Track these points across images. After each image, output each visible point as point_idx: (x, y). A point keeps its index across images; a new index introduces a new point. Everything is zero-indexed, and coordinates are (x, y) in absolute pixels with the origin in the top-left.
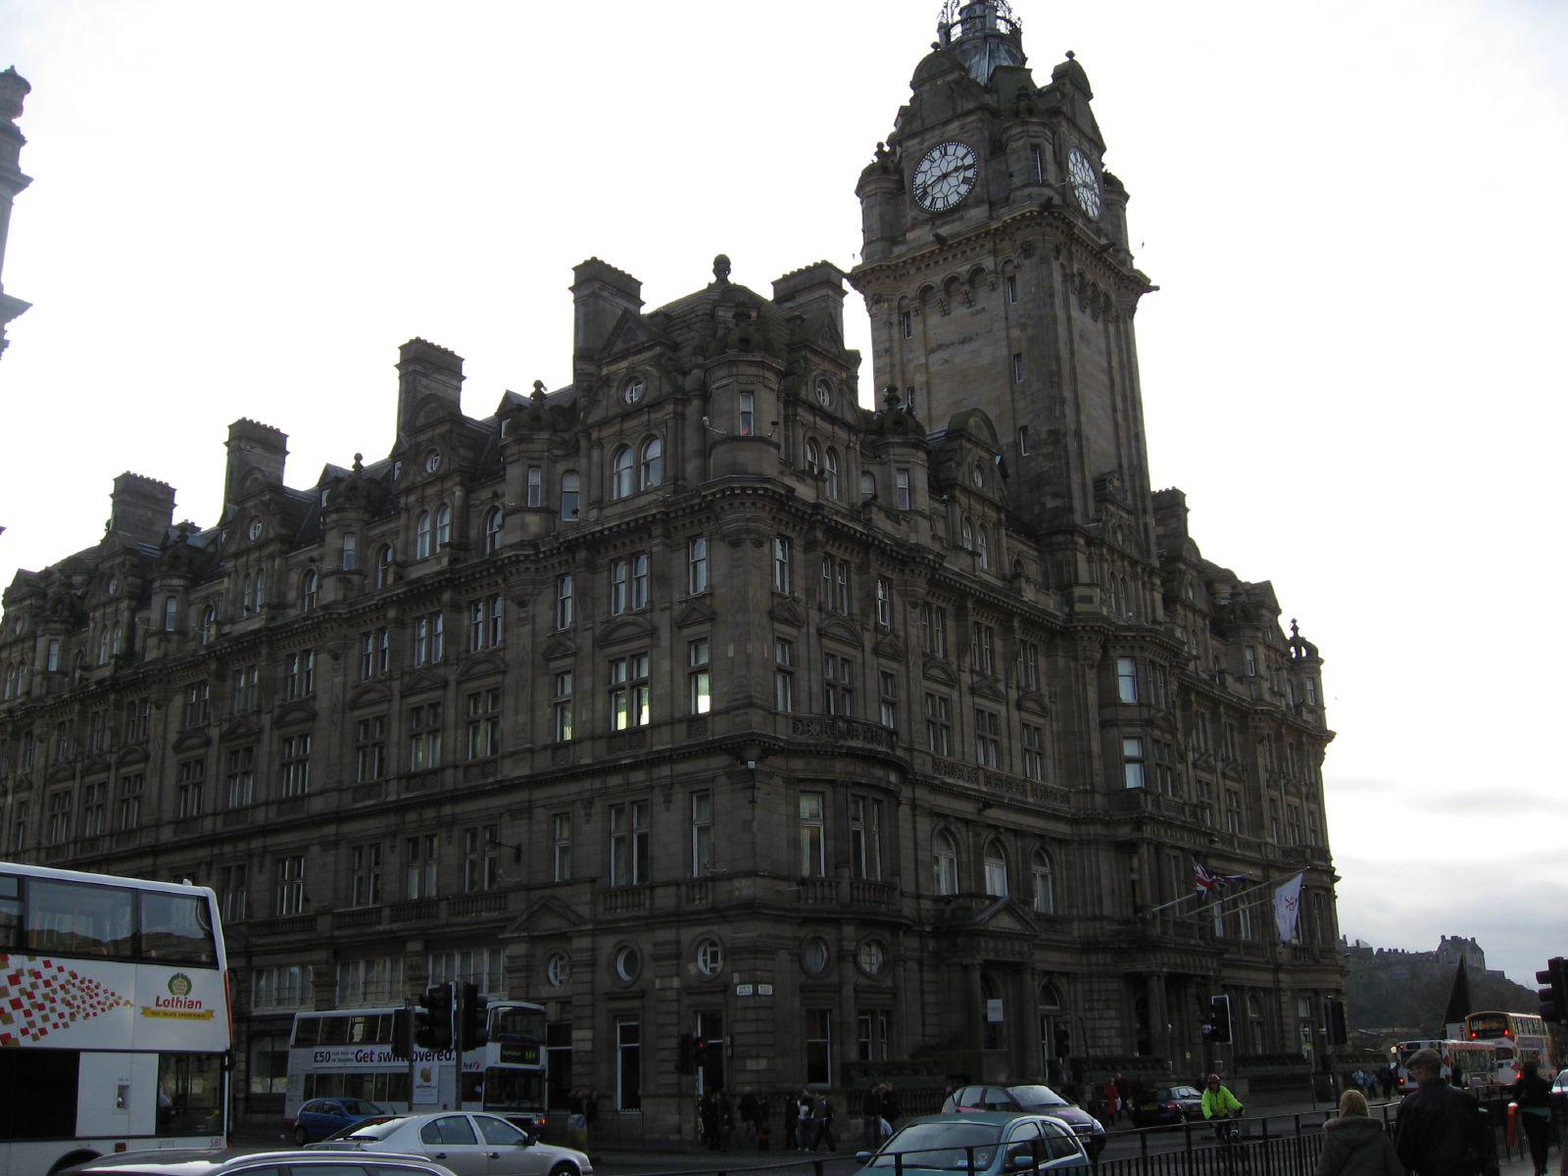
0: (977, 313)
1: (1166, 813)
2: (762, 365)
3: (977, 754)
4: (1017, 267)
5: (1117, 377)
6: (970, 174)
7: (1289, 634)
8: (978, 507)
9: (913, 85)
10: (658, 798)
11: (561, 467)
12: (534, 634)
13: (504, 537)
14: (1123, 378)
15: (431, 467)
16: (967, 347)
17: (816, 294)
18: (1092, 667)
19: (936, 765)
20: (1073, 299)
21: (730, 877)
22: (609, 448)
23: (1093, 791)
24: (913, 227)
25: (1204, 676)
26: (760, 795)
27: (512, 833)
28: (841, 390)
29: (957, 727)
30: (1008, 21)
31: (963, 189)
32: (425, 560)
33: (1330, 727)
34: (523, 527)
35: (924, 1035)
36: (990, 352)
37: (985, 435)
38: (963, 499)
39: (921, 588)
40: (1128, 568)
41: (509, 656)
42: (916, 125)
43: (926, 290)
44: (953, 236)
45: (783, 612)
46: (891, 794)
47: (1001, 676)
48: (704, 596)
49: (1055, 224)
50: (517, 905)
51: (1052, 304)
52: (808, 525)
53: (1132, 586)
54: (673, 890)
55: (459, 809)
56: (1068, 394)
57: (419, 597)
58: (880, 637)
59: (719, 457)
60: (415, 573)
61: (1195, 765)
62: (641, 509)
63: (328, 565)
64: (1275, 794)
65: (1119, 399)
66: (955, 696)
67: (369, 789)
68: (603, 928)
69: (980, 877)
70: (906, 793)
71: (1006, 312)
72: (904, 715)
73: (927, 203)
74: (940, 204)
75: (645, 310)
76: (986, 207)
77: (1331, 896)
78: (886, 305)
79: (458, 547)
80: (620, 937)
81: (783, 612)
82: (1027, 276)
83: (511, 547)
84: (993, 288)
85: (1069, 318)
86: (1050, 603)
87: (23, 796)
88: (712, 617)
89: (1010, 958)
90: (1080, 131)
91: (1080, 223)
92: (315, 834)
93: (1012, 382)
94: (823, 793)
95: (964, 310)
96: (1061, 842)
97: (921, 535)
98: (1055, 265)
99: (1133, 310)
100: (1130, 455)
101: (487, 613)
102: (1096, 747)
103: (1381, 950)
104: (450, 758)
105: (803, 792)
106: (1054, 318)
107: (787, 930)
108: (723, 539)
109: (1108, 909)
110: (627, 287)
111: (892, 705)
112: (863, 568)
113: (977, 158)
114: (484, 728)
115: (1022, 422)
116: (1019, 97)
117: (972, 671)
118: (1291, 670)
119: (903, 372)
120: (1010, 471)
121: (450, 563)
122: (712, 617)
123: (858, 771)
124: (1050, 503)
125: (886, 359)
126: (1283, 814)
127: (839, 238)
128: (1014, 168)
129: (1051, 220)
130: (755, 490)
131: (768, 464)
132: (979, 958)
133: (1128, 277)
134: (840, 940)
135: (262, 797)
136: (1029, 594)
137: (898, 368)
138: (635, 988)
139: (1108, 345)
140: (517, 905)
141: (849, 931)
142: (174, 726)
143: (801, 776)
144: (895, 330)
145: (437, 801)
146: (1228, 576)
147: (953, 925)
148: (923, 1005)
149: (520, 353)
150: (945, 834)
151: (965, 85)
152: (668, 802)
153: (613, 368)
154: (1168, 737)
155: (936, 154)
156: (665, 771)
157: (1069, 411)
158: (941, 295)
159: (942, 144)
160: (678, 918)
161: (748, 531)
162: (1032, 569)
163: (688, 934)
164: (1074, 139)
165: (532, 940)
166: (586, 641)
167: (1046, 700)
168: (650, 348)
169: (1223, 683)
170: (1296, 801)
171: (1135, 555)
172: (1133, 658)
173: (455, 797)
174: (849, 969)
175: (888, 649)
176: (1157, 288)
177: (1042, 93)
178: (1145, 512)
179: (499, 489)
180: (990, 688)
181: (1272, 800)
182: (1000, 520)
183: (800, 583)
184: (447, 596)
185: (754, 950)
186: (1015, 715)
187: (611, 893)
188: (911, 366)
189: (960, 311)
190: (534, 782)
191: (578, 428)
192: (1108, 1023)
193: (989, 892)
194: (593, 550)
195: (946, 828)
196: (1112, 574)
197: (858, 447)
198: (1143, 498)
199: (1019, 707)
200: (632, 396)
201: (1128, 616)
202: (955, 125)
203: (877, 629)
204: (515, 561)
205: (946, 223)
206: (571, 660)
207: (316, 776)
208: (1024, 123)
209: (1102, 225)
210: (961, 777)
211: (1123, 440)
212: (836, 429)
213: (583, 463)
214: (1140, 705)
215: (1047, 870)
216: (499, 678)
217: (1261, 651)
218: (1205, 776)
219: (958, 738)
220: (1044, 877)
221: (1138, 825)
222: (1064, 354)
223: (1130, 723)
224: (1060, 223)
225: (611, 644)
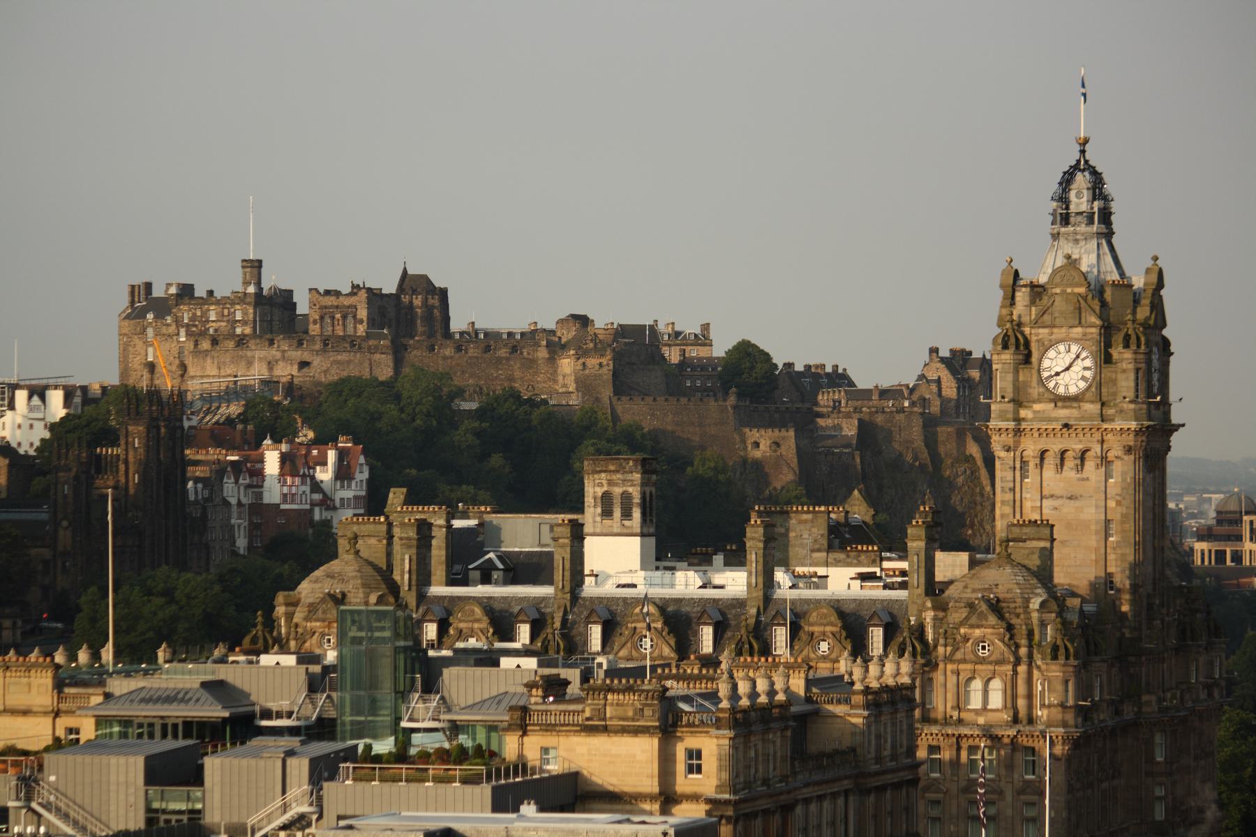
24: (1039, 401)
36: (1091, 513)
74: (1061, 391)
95: (1073, 474)
103: (789, 365)
137: (1018, 504)
144: (1018, 474)
155: (1061, 347)
189: (1069, 472)
202: (1079, 330)
205: (1064, 407)
206: (941, 795)
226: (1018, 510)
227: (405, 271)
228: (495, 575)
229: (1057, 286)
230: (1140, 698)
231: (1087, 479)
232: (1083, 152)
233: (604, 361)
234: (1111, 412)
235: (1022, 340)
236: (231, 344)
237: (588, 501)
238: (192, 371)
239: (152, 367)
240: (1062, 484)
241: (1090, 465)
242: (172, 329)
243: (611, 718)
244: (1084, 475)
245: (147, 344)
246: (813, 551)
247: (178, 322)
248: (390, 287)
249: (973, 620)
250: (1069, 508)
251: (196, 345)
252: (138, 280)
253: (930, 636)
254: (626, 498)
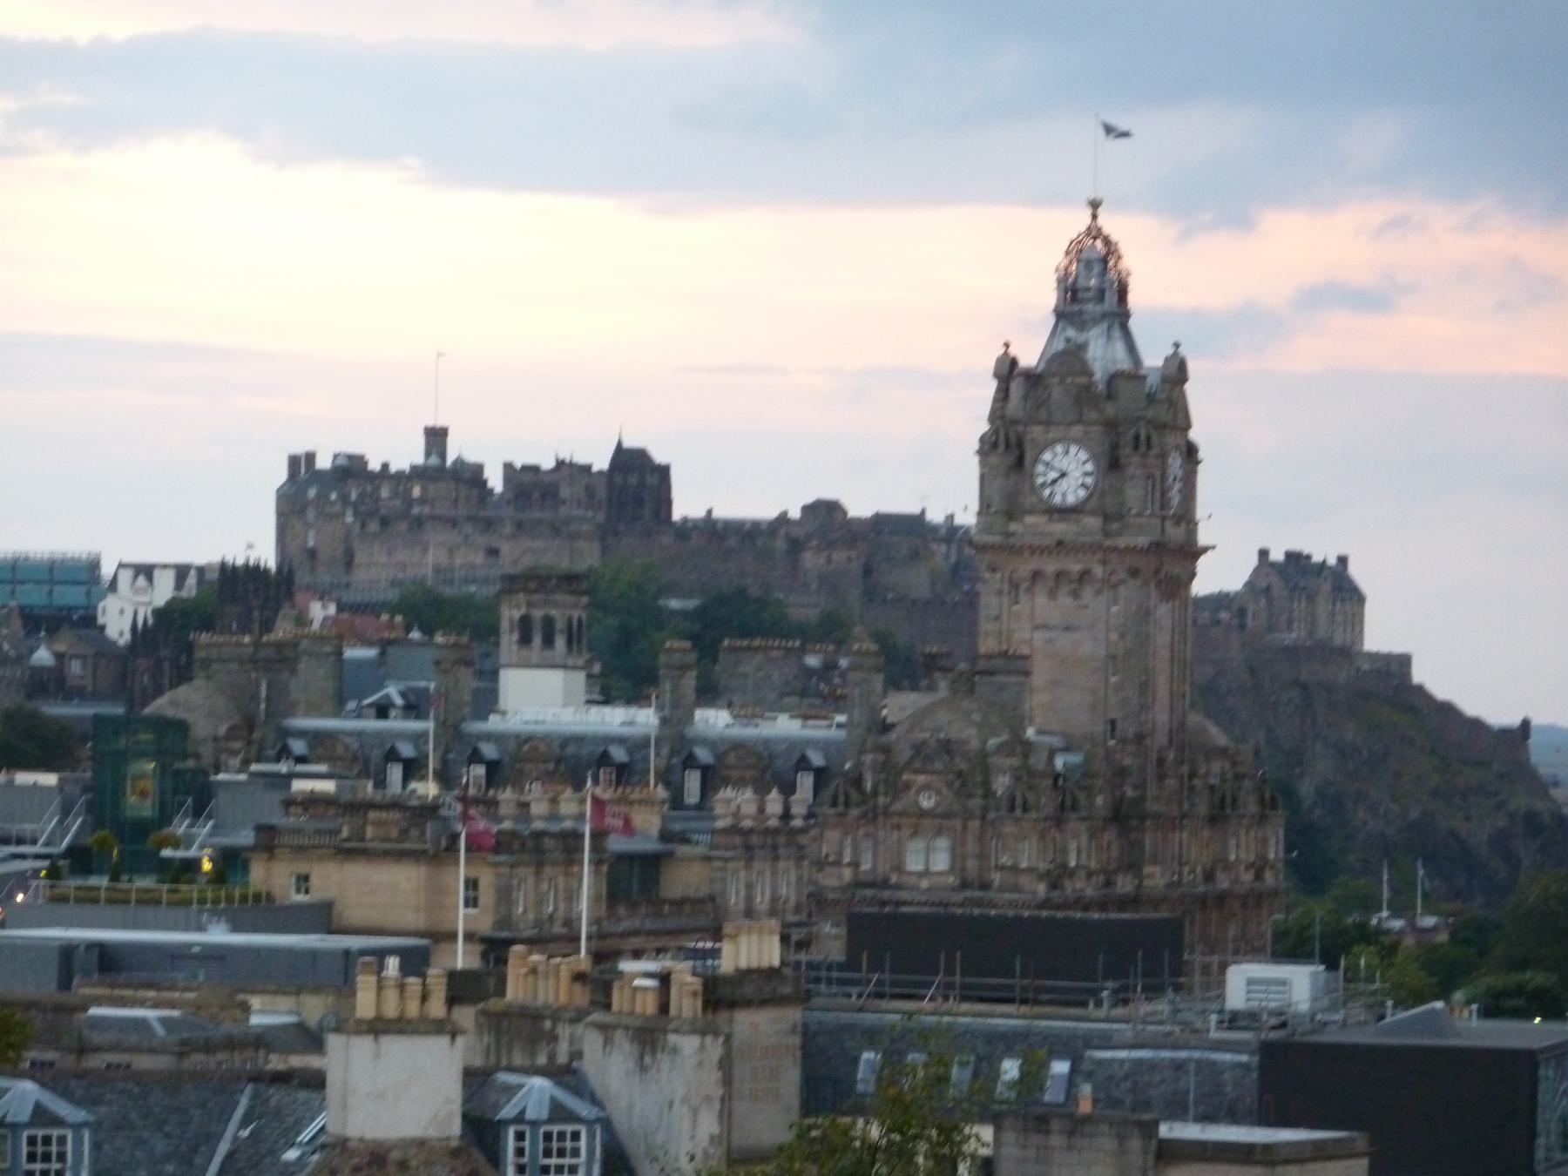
24: (1031, 512)
34: (840, 877)
36: (1089, 646)
43: (1036, 575)
73: (1047, 492)
74: (1057, 499)
78: (998, 575)
84: (1099, 592)
113: (1097, 467)
115: (1112, 715)
144: (1005, 600)
155: (1059, 449)
158: (1051, 584)
159: (1066, 440)
189: (1065, 600)
200: (927, 802)
227: (619, 444)
228: (393, 713)
229: (1055, 374)
230: (1141, 870)
232: (1094, 217)
233: (853, 554)
234: (1115, 526)
235: (1013, 440)
236: (403, 526)
237: (505, 625)
238: (360, 558)
239: (312, 554)
241: (1088, 592)
242: (337, 508)
243: (372, 840)
244: (1084, 602)
245: (308, 526)
246: (783, 695)
247: (344, 499)
248: (601, 463)
249: (917, 764)
250: (1064, 641)
251: (363, 526)
252: (300, 449)
253: (869, 785)
254: (548, 623)
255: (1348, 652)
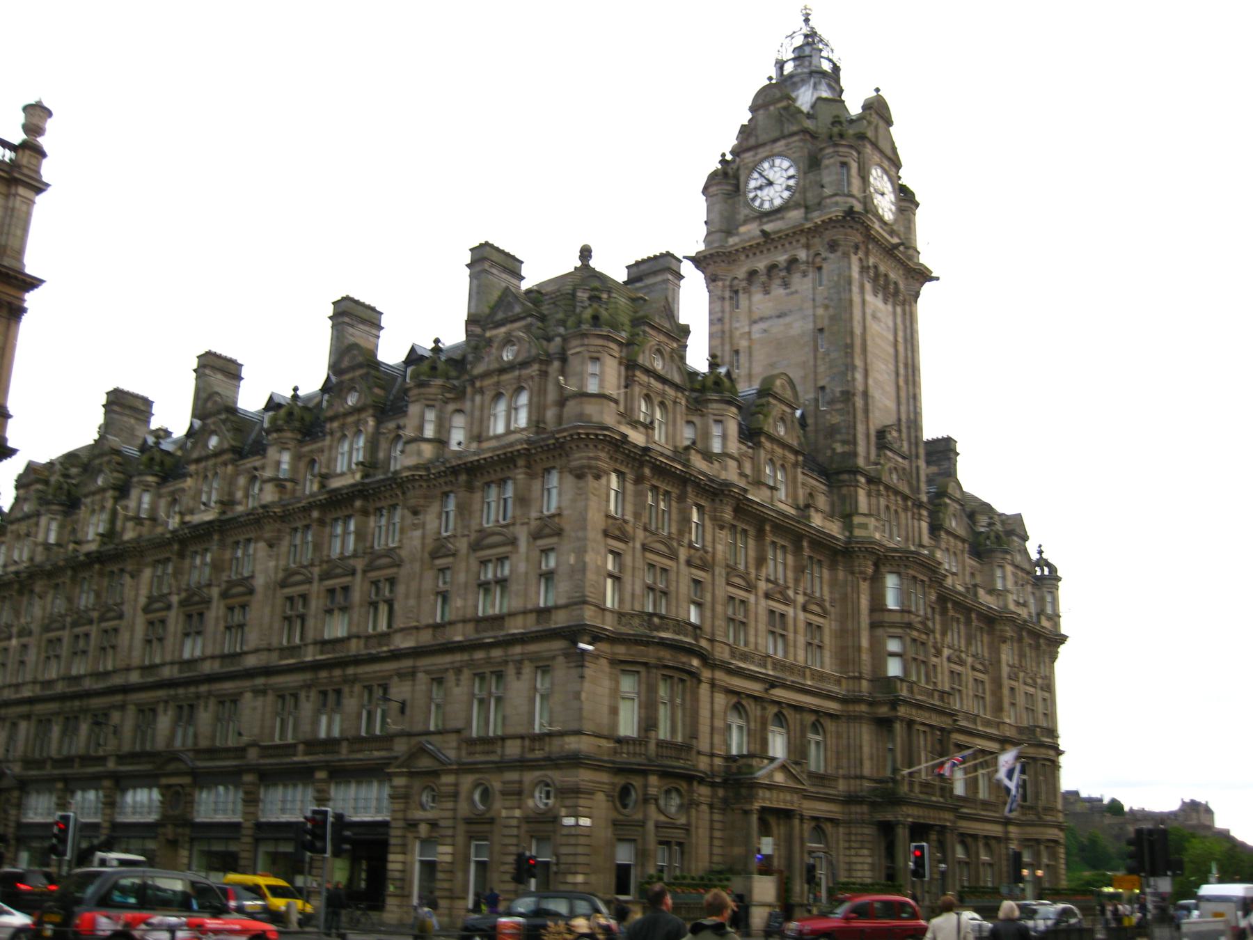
0: (792, 293)
1: (919, 697)
2: (608, 338)
3: (768, 646)
4: (825, 259)
5: (901, 348)
6: (791, 183)
7: (1034, 556)
8: (779, 451)
9: (753, 109)
10: (511, 670)
11: (451, 407)
12: (424, 537)
13: (402, 460)
14: (906, 349)
15: (352, 400)
16: (781, 321)
17: (659, 278)
18: (865, 580)
19: (733, 655)
20: (868, 286)
21: (562, 734)
22: (489, 395)
23: (860, 678)
24: (745, 222)
25: (960, 588)
26: (588, 672)
27: (400, 691)
28: (672, 357)
29: (752, 624)
30: (830, 60)
31: (786, 194)
32: (342, 474)
33: (1063, 631)
34: (419, 453)
35: (711, 862)
36: (800, 326)
37: (788, 394)
38: (768, 445)
39: (728, 515)
40: (900, 502)
41: (404, 553)
42: (752, 141)
43: (753, 274)
44: (775, 233)
45: (616, 531)
46: (695, 676)
47: (791, 584)
48: (553, 516)
49: (856, 226)
50: (401, 747)
51: (850, 291)
52: (639, 464)
53: (902, 515)
54: (518, 742)
55: (361, 670)
56: (858, 362)
57: (337, 503)
58: (692, 551)
59: (571, 407)
60: (335, 484)
61: (949, 659)
62: (511, 445)
63: (268, 473)
64: (1014, 683)
65: (901, 366)
66: (752, 598)
67: (292, 650)
68: (464, 768)
69: (764, 743)
70: (706, 674)
71: (814, 294)
72: (708, 614)
74: (767, 206)
75: (525, 286)
76: (802, 210)
77: (1055, 766)
78: (720, 283)
79: (369, 466)
80: (477, 776)
81: (616, 531)
82: (832, 264)
83: (409, 468)
84: (805, 274)
85: (864, 302)
86: (834, 528)
87: (24, 640)
88: (559, 533)
89: (782, 806)
90: (881, 152)
91: (877, 226)
92: (247, 683)
93: (816, 350)
94: (638, 672)
95: (781, 291)
96: (832, 716)
97: (730, 473)
98: (854, 260)
99: (917, 295)
100: (908, 412)
101: (389, 520)
102: (865, 643)
104: (354, 630)
105: (624, 672)
106: (851, 301)
107: (604, 777)
108: (571, 471)
109: (867, 771)
110: (511, 265)
111: (699, 605)
112: (681, 498)
113: (798, 170)
114: (383, 610)
115: (821, 383)
116: (833, 124)
117: (768, 580)
118: (1035, 585)
119: (731, 337)
120: (810, 421)
121: (363, 477)
122: (559, 533)
123: (667, 656)
124: (839, 448)
125: (718, 327)
126: (1021, 700)
127: (684, 229)
128: (826, 180)
129: (852, 224)
130: (597, 435)
131: (608, 416)
132: (757, 805)
133: (914, 270)
134: (646, 786)
135: (209, 652)
136: (817, 521)
137: (727, 335)
138: (488, 816)
139: (895, 324)
140: (401, 747)
141: (653, 780)
142: (144, 592)
143: (622, 658)
144: (727, 303)
145: (342, 663)
146: (987, 508)
147: (736, 781)
148: (712, 838)
149: (425, 315)
150: (738, 708)
151: (792, 112)
152: (519, 673)
153: (494, 332)
154: (924, 637)
155: (766, 165)
156: (518, 649)
157: (859, 376)
158: (763, 278)
159: (771, 157)
160: (522, 764)
161: (590, 467)
162: (822, 501)
163: (529, 777)
164: (876, 157)
165: (411, 775)
166: (462, 545)
167: (827, 605)
168: (523, 318)
169: (976, 594)
170: (1031, 690)
171: (907, 491)
172: (899, 574)
173: (357, 661)
174: (652, 808)
175: (699, 562)
176: (937, 279)
177: (852, 121)
178: (917, 457)
179: (401, 422)
180: (781, 593)
181: (1012, 689)
182: (797, 461)
183: (629, 508)
184: (358, 504)
185: (576, 791)
186: (802, 616)
187: (471, 742)
188: (737, 333)
189: (778, 291)
190: (417, 652)
191: (467, 377)
192: (860, 860)
193: (771, 754)
194: (472, 473)
195: (739, 703)
196: (887, 507)
197: (683, 402)
198: (917, 445)
199: (805, 609)
200: (508, 355)
201: (896, 541)
202: (782, 143)
203: (690, 546)
204: (412, 479)
206: (450, 559)
207: (253, 638)
208: (836, 145)
209: (895, 228)
210: (753, 663)
211: (903, 400)
212: (667, 388)
213: (467, 406)
214: (902, 611)
215: (819, 738)
216: (394, 570)
217: (1009, 569)
218: (957, 668)
219: (752, 632)
220: (818, 743)
221: (894, 704)
222: (858, 330)
223: (893, 625)
224: (859, 226)
225: (482, 549)
226: (727, 340)
231: (796, 292)
232: (807, 20)
240: (771, 304)
241: (796, 279)
244: (793, 289)
250: (777, 327)
255: (1210, 827)
